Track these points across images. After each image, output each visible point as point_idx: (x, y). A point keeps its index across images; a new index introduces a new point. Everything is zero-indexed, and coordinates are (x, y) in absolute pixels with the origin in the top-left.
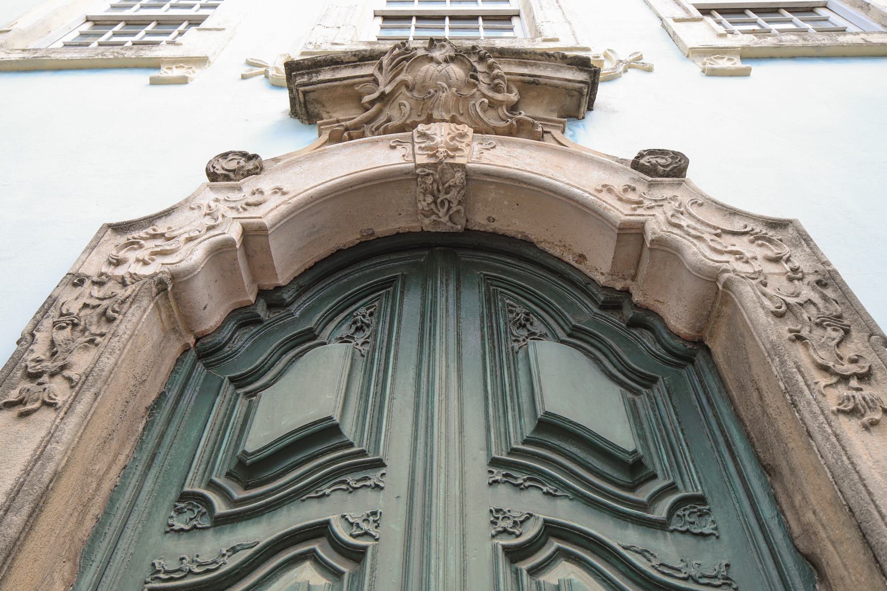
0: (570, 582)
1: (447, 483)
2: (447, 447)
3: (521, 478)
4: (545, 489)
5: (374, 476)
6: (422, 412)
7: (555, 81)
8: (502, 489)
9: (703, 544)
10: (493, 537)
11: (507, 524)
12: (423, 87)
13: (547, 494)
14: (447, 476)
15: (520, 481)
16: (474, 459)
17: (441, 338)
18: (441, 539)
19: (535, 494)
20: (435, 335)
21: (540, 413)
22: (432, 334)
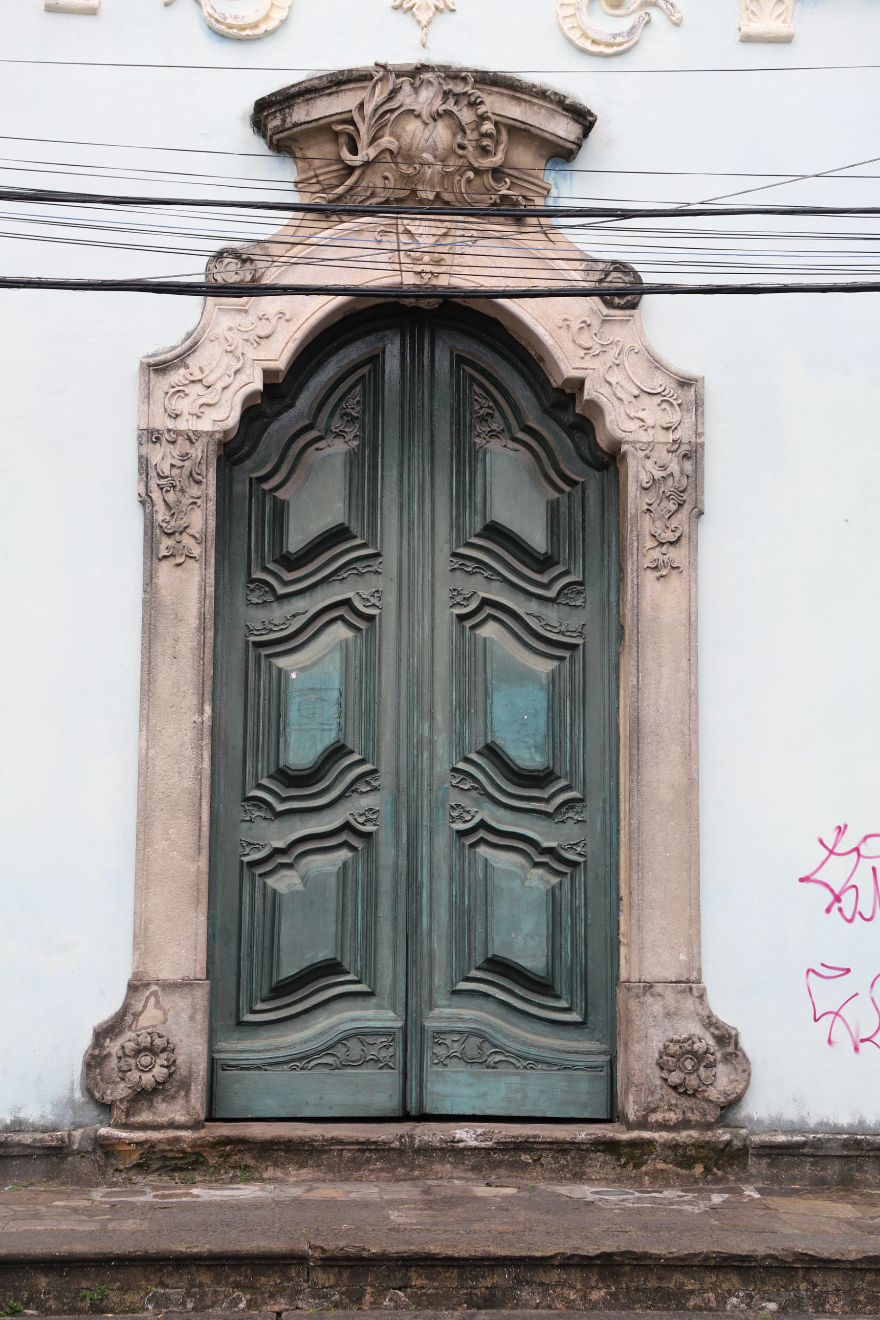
0: (492, 639)
1: (423, 572)
2: (423, 545)
3: (471, 566)
4: (486, 574)
5: (375, 564)
6: (405, 513)
7: (547, 135)
8: (458, 573)
9: (574, 611)
10: (451, 607)
11: (459, 599)
12: (409, 155)
13: (487, 578)
14: (423, 568)
15: (469, 569)
16: (441, 551)
17: (419, 442)
18: (420, 612)
19: (479, 577)
20: (414, 439)
21: (488, 520)
22: (411, 439)
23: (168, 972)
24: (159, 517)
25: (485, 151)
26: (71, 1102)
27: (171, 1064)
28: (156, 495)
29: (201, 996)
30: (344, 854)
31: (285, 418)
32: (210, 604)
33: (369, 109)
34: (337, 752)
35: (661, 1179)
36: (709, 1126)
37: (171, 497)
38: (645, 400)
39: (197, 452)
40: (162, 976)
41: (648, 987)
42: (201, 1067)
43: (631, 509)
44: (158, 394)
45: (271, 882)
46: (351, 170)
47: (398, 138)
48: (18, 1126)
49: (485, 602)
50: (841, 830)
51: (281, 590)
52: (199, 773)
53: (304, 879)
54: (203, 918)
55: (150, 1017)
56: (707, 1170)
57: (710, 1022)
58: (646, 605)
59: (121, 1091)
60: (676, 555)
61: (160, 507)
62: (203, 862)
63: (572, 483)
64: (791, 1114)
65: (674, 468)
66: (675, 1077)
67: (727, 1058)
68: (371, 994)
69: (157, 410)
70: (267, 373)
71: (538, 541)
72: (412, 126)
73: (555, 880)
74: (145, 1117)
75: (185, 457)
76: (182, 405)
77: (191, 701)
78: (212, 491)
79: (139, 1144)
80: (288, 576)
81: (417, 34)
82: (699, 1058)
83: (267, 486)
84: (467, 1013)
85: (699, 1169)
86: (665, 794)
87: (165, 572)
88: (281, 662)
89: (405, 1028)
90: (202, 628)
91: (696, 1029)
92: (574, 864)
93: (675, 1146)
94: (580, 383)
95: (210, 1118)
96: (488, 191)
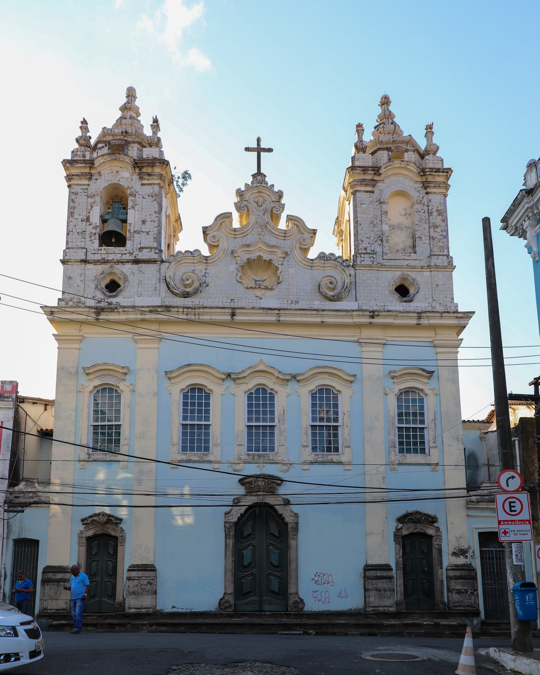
23: (229, 592)
24: (227, 533)
25: (269, 485)
26: (217, 608)
27: (230, 604)
28: (226, 530)
29: (233, 595)
30: (251, 577)
31: (243, 519)
32: (234, 544)
33: (254, 480)
34: (250, 563)
35: (293, 618)
36: (299, 611)
37: (228, 530)
38: (291, 517)
39: (232, 524)
40: (228, 592)
41: (291, 594)
42: (233, 604)
43: (289, 531)
44: (227, 517)
45: (242, 581)
46: (252, 487)
47: (257, 483)
48: (210, 611)
49: (270, 543)
50: (317, 573)
51: (243, 542)
52: (232, 566)
53: (246, 580)
54: (233, 585)
55: (227, 598)
56: (299, 617)
57: (299, 598)
58: (291, 543)
59: (223, 607)
60: (295, 537)
61: (227, 532)
62: (233, 578)
63: (282, 527)
64: (310, 610)
65: (294, 525)
66: (295, 605)
67: (302, 603)
68: (255, 595)
69: (227, 519)
70: (241, 514)
71: (277, 535)
72: (259, 482)
73: (280, 580)
74: (226, 610)
75: (230, 525)
76: (230, 518)
77: (231, 557)
78: (234, 530)
79: (226, 614)
80: (244, 540)
81: (260, 470)
82: (298, 603)
83: (241, 528)
84: (268, 598)
85: (298, 617)
86: (293, 569)
87: (228, 540)
88: (243, 551)
89: (260, 600)
90: (232, 548)
91: (298, 599)
92: (282, 578)
93: (294, 614)
94: (282, 514)
95: (234, 611)
96: (269, 489)
